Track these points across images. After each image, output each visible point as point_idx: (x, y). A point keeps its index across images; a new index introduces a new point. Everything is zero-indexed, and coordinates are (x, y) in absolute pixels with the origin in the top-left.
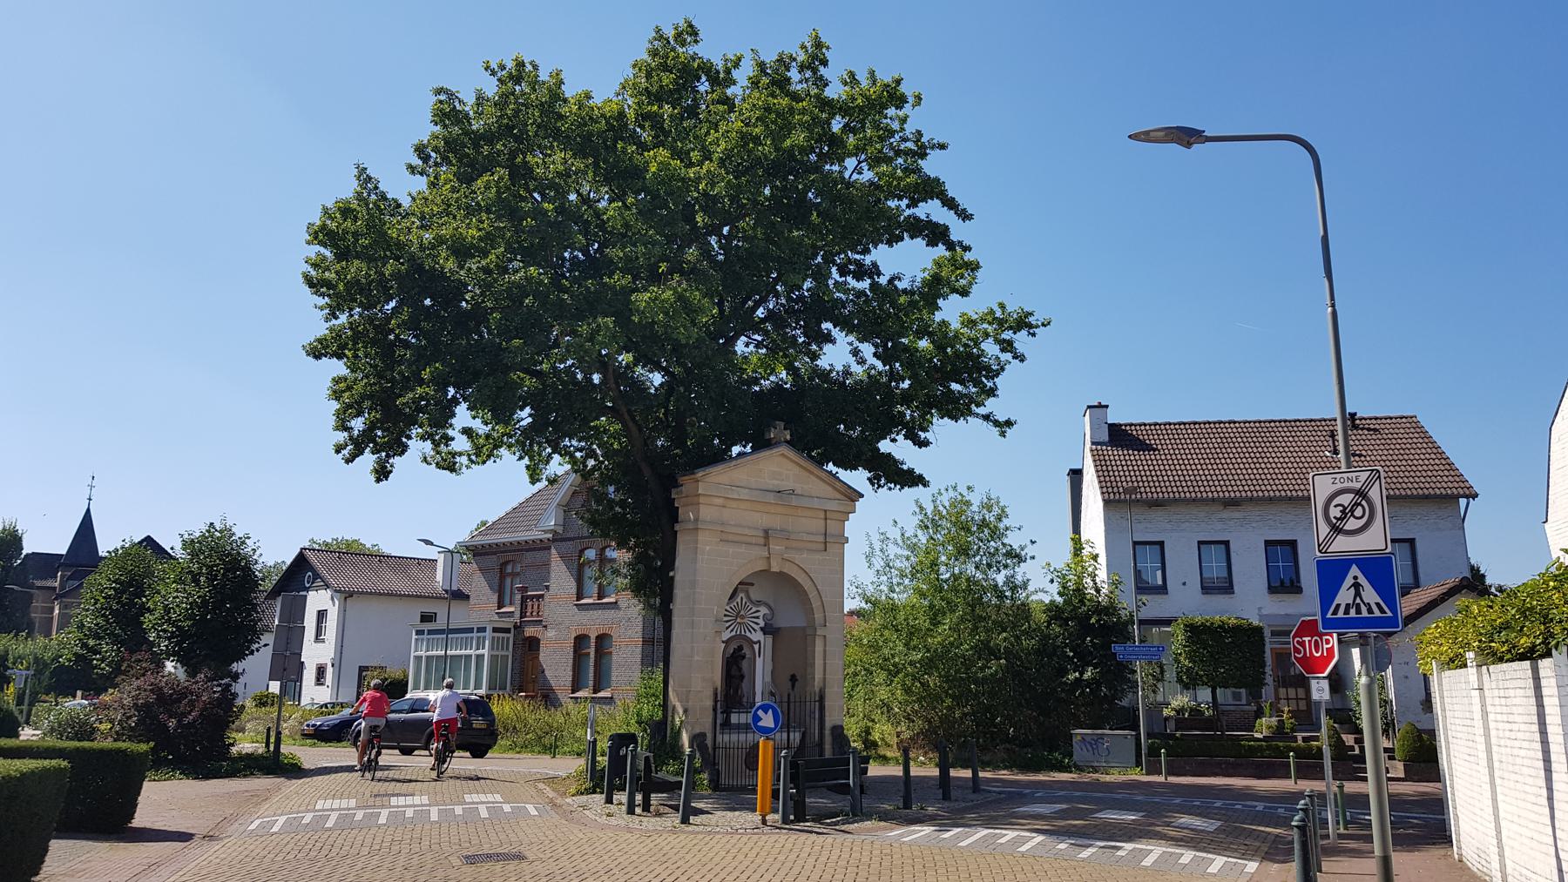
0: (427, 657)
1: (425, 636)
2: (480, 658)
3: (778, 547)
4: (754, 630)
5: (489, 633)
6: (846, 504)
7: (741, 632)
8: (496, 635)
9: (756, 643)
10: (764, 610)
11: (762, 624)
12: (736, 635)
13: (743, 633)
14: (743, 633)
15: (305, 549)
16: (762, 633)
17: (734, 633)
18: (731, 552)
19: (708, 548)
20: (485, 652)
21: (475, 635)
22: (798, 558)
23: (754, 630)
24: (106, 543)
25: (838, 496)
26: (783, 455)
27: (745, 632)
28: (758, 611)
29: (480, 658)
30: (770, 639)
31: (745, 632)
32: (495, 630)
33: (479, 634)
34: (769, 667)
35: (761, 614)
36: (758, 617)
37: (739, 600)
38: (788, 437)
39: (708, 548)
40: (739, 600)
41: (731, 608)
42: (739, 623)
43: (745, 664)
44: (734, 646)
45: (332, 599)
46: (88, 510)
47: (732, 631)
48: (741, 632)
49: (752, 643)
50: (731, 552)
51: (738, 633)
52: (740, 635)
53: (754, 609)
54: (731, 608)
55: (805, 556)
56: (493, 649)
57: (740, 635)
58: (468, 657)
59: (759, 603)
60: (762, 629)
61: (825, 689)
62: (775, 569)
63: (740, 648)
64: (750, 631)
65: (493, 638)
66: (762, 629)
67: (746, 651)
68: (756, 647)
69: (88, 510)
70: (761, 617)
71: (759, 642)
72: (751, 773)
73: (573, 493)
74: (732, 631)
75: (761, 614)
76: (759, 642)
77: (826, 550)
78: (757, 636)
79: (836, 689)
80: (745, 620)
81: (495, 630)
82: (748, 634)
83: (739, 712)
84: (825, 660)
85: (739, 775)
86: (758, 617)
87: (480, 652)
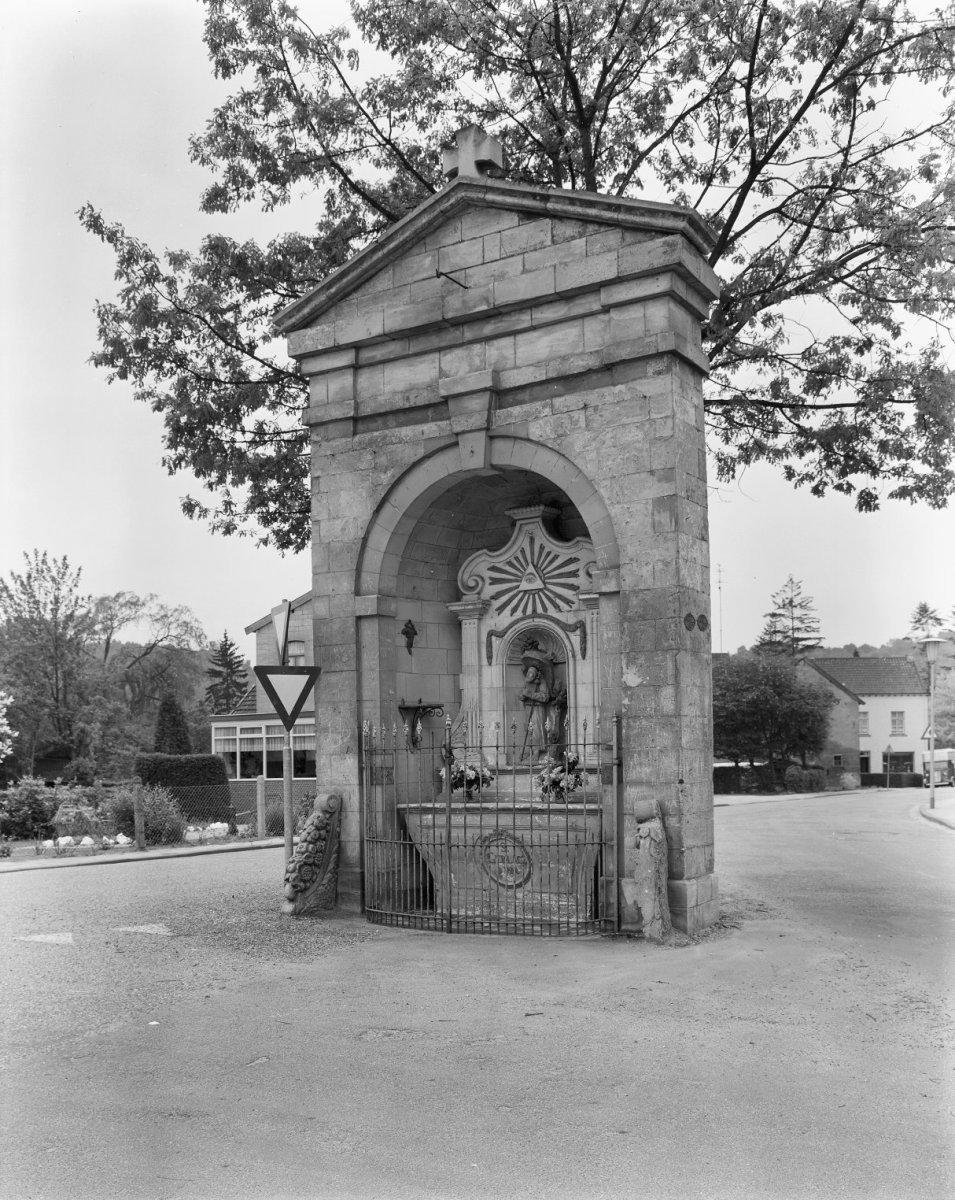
4: (568, 602)
13: (540, 610)
14: (540, 610)
23: (568, 602)
28: (571, 561)
31: (545, 609)
36: (574, 574)
42: (526, 592)
47: (514, 610)
64: (557, 607)
70: (582, 573)
76: (581, 626)
86: (574, 574)
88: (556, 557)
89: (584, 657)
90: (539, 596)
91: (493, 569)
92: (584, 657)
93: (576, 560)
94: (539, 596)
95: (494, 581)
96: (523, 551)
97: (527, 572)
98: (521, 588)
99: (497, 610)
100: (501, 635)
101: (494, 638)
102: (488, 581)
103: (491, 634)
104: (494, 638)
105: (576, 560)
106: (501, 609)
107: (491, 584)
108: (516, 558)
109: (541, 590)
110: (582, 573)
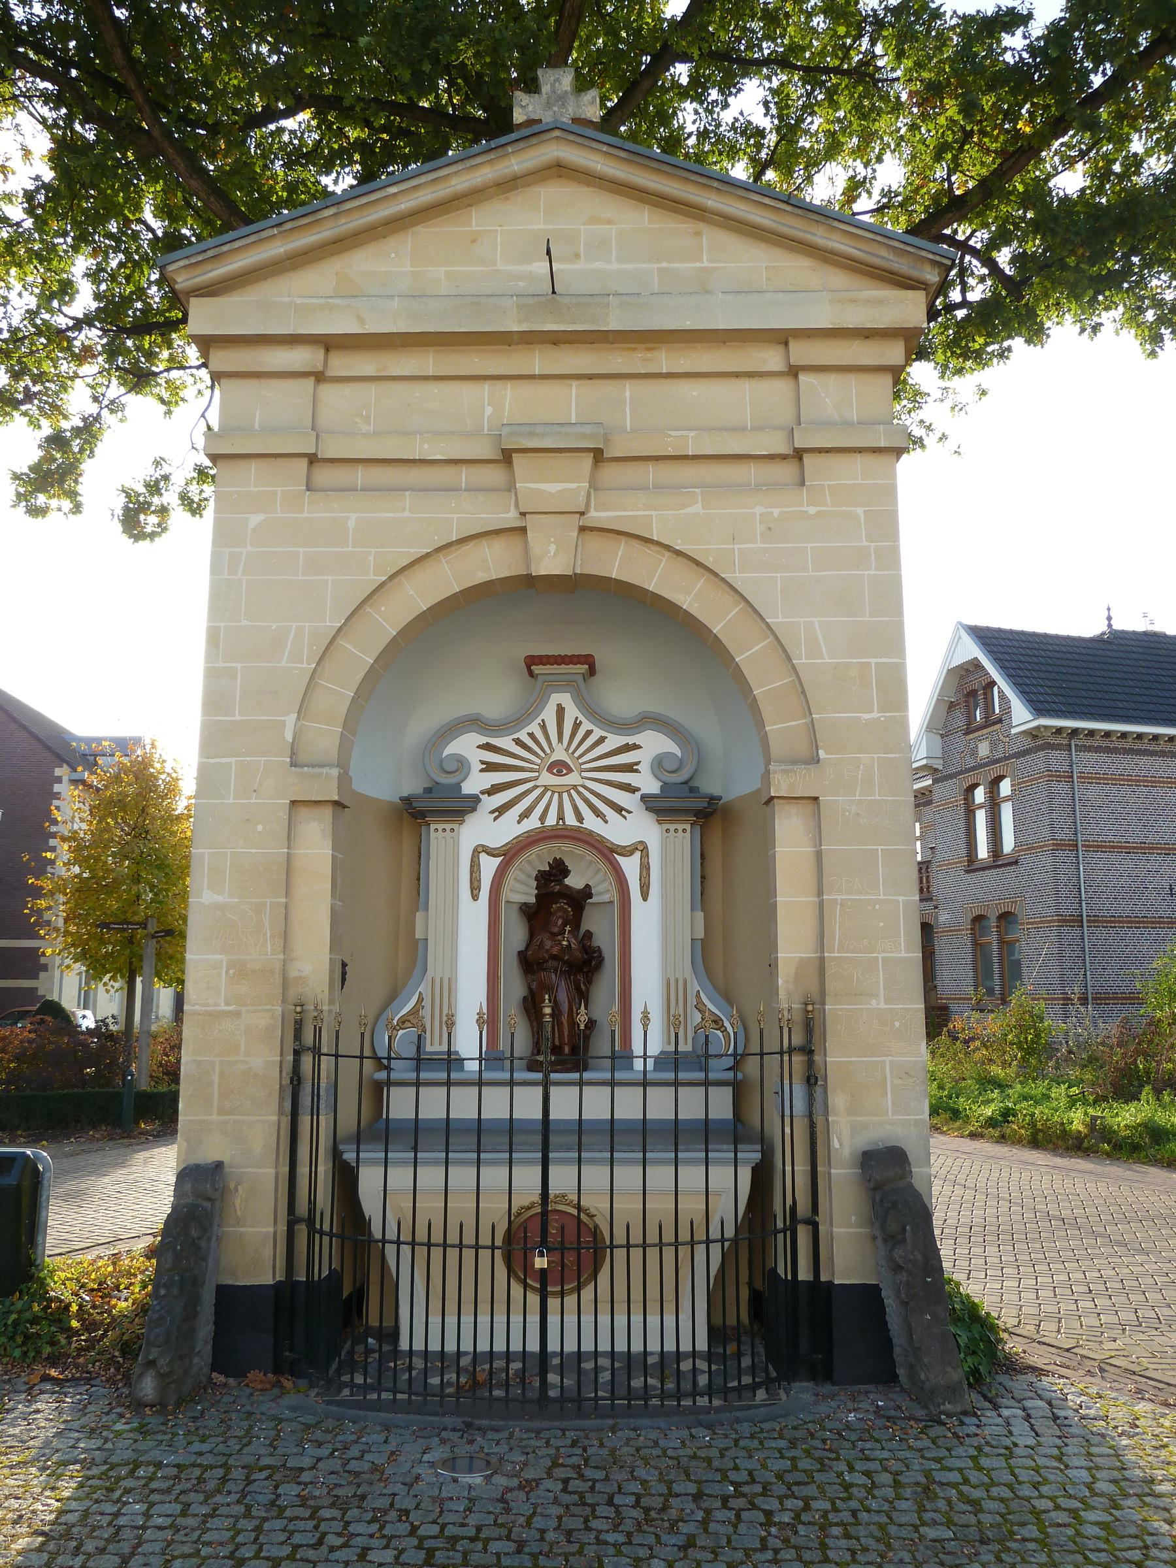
3: (553, 488)
4: (619, 809)
6: (868, 301)
7: (561, 817)
9: (628, 851)
11: (649, 784)
13: (571, 820)
17: (532, 823)
18: (351, 524)
23: (619, 809)
26: (559, 170)
27: (580, 818)
28: (628, 748)
30: (683, 836)
31: (580, 818)
34: (691, 925)
36: (630, 768)
40: (549, 715)
41: (518, 742)
42: (546, 788)
43: (597, 924)
44: (538, 859)
47: (525, 815)
48: (561, 817)
49: (607, 852)
50: (351, 524)
51: (551, 820)
53: (614, 741)
54: (518, 742)
55: (697, 508)
60: (644, 798)
61: (823, 994)
63: (559, 870)
64: (598, 813)
68: (630, 866)
70: (644, 768)
74: (525, 815)
76: (641, 848)
77: (802, 483)
79: (879, 1004)
80: (573, 779)
82: (591, 823)
84: (820, 893)
86: (630, 768)
88: (602, 740)
89: (645, 897)
90: (570, 796)
91: (487, 747)
92: (645, 898)
93: (636, 747)
94: (570, 796)
95: (490, 767)
96: (543, 727)
98: (538, 783)
99: (492, 812)
100: (492, 853)
101: (483, 856)
102: (476, 766)
103: (478, 850)
104: (483, 856)
105: (636, 747)
106: (501, 810)
107: (482, 771)
108: (531, 735)
109: (575, 787)
110: (644, 768)
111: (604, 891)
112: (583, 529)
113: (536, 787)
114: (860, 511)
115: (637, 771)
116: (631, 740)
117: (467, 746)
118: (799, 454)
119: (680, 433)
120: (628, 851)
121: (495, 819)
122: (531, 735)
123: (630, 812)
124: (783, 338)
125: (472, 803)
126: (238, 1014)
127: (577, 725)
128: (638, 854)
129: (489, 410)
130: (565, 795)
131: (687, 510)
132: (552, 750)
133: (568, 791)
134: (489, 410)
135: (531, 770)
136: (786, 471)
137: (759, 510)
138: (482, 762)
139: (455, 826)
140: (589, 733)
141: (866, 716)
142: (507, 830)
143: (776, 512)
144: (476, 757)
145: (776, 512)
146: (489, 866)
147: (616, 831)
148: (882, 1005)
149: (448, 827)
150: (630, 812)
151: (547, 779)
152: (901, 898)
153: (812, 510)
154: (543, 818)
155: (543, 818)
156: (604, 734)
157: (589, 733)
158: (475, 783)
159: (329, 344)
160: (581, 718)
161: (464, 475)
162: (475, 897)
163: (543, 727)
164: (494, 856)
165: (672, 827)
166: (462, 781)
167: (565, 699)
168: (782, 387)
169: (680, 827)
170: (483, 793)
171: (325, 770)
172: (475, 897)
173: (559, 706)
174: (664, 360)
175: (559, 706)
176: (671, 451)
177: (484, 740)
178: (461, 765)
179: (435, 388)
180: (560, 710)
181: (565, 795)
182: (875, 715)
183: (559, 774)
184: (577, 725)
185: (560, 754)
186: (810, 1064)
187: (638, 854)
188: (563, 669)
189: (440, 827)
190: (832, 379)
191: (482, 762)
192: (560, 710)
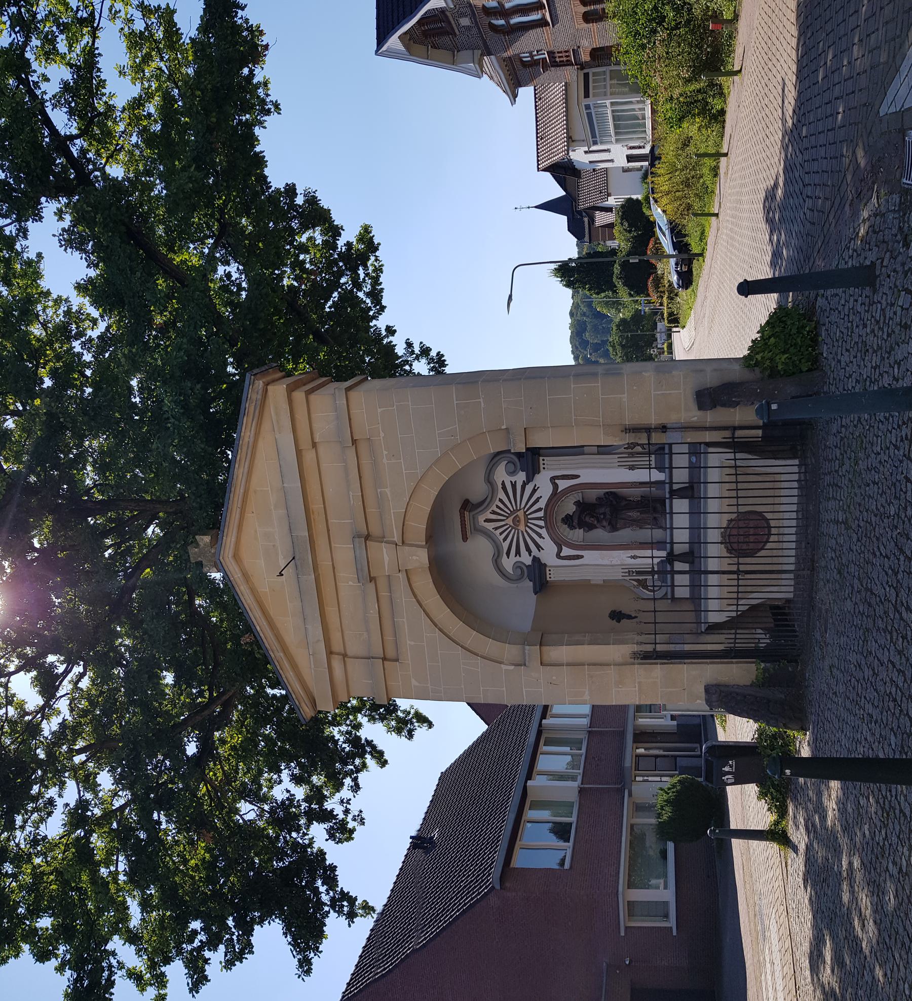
0: (616, 134)
1: (598, 139)
2: (612, 104)
4: (534, 491)
5: (590, 101)
8: (591, 95)
9: (556, 486)
10: (501, 474)
11: (521, 477)
12: (546, 527)
13: (541, 514)
14: (541, 514)
15: (538, 168)
16: (537, 476)
17: (543, 532)
19: (414, 682)
20: (608, 102)
21: (593, 111)
22: (394, 510)
23: (534, 491)
24: (556, 192)
25: (266, 426)
27: (540, 510)
28: (504, 488)
29: (612, 104)
31: (540, 510)
32: (587, 95)
33: (592, 108)
35: (508, 480)
36: (514, 486)
37: (490, 526)
38: (207, 539)
39: (414, 682)
40: (490, 526)
41: (505, 540)
43: (592, 495)
45: (574, 151)
46: (536, 207)
49: (556, 495)
51: (542, 523)
52: (544, 518)
53: (501, 495)
54: (505, 540)
55: (388, 491)
56: (605, 95)
57: (544, 518)
58: (613, 111)
59: (489, 480)
62: (420, 557)
65: (594, 96)
66: (530, 479)
67: (569, 507)
68: (563, 485)
69: (536, 207)
71: (553, 479)
72: (772, 538)
73: (436, 48)
75: (508, 480)
76: (553, 479)
78: (543, 485)
80: (521, 514)
81: (587, 95)
82: (542, 504)
83: (671, 513)
85: (775, 560)
86: (514, 486)
87: (608, 105)
88: (501, 500)
89: (577, 477)
91: (508, 554)
92: (577, 477)
93: (503, 483)
95: (518, 553)
96: (496, 529)
97: (512, 524)
99: (539, 551)
100: (560, 550)
101: (562, 555)
102: (518, 559)
104: (562, 555)
105: (503, 483)
106: (539, 547)
108: (501, 534)
109: (525, 512)
111: (578, 496)
112: (403, 542)
113: (526, 531)
114: (379, 410)
115: (515, 482)
116: (500, 486)
117: (508, 563)
118: (354, 442)
119: (351, 499)
120: (556, 486)
121: (543, 549)
122: (501, 534)
123: (535, 485)
124: (299, 453)
125: (536, 560)
126: (640, 683)
127: (494, 513)
128: (557, 481)
129: (351, 583)
130: (529, 517)
131: (389, 496)
132: (507, 524)
133: (527, 515)
134: (351, 583)
135: (518, 533)
136: (363, 448)
137: (385, 461)
138: (516, 556)
139: (548, 569)
140: (497, 507)
141: (482, 404)
142: (548, 545)
143: (385, 453)
144: (513, 559)
145: (385, 453)
146: (566, 551)
147: (545, 491)
148: (626, 395)
149: (548, 572)
150: (535, 485)
151: (522, 527)
152: (572, 386)
153: (382, 434)
154: (541, 527)
155: (541, 527)
156: (498, 499)
157: (497, 507)
158: (527, 560)
159: (330, 653)
160: (490, 511)
161: (384, 594)
162: (582, 557)
163: (496, 529)
164: (562, 549)
165: (542, 466)
166: (525, 565)
167: (481, 519)
168: (321, 449)
169: (541, 462)
170: (530, 555)
171: (526, 651)
172: (582, 557)
173: (485, 521)
174: (316, 506)
175: (485, 521)
176: (361, 503)
177: (505, 555)
178: (518, 566)
179: (343, 606)
180: (487, 521)
181: (529, 517)
182: (481, 400)
183: (519, 521)
184: (494, 513)
185: (510, 521)
186: (656, 429)
187: (557, 481)
188: (467, 523)
189: (548, 576)
190: (315, 425)
191: (516, 556)
192: (487, 521)
